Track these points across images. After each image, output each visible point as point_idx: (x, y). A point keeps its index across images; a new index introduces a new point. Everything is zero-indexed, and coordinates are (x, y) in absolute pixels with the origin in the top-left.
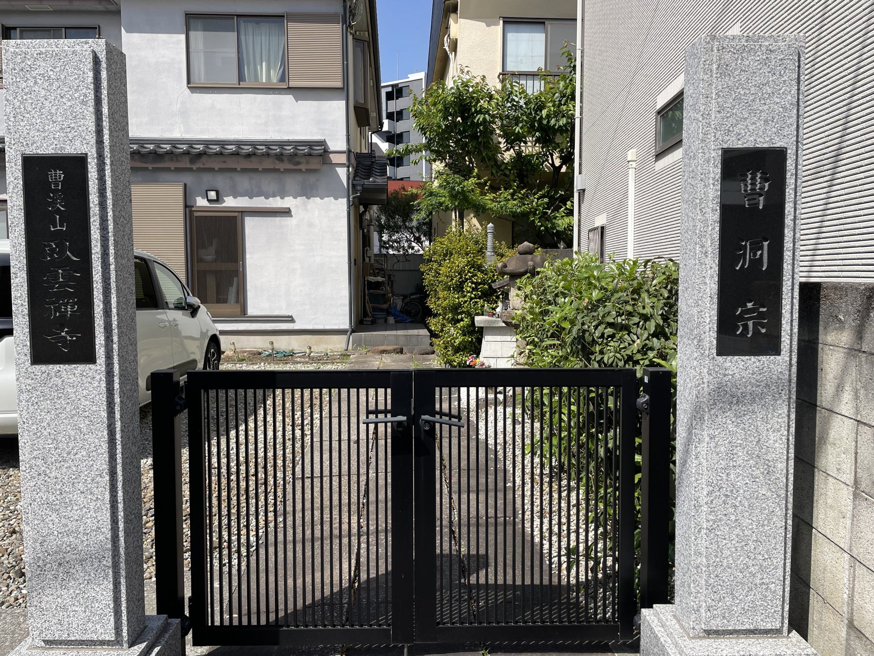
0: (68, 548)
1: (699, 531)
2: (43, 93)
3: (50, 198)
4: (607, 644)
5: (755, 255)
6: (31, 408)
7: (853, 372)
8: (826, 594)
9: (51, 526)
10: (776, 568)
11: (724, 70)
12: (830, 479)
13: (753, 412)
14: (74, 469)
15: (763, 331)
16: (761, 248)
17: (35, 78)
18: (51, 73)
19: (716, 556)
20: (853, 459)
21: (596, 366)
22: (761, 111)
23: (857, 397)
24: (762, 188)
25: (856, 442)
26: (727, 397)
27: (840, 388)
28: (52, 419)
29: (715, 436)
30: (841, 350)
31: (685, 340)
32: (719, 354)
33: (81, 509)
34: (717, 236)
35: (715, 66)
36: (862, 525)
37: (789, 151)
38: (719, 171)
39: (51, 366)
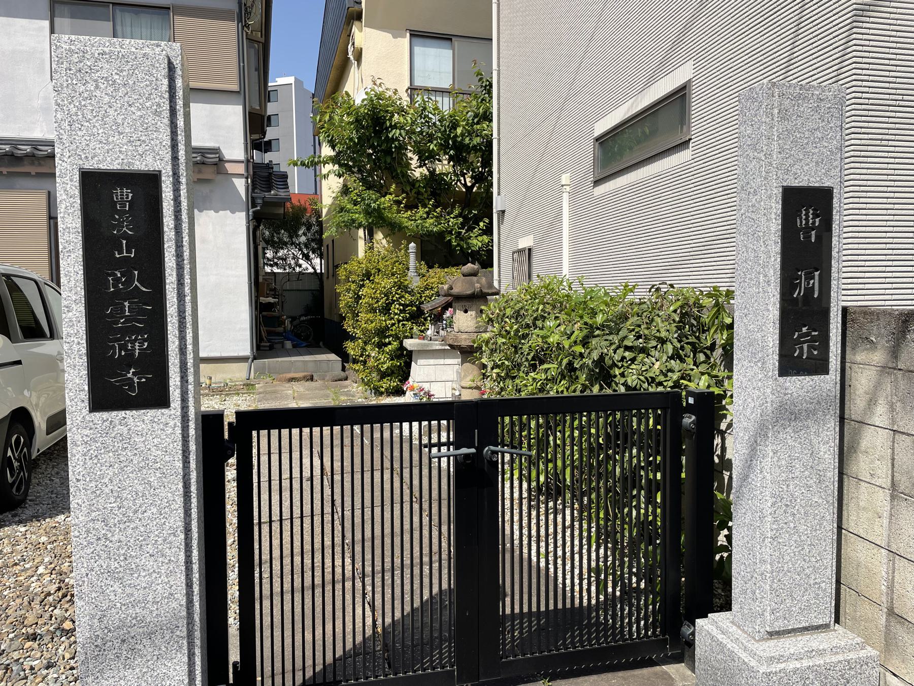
0: (134, 622)
1: (764, 540)
2: (107, 99)
3: (115, 220)
4: (650, 658)
5: (809, 284)
6: (89, 463)
7: (888, 387)
8: (861, 588)
9: (112, 597)
10: (826, 568)
11: (784, 115)
12: (863, 484)
13: (808, 427)
14: (142, 529)
15: (816, 353)
16: (813, 278)
17: (96, 81)
18: (117, 77)
19: (779, 562)
20: (890, 465)
21: (622, 390)
22: (813, 154)
23: (892, 408)
24: (814, 223)
25: (893, 449)
26: (788, 415)
27: (872, 402)
28: (115, 474)
29: (777, 451)
30: (873, 368)
31: (745, 363)
32: (781, 374)
33: (150, 575)
34: (778, 267)
35: (776, 111)
36: (902, 523)
37: (835, 191)
38: (780, 206)
39: (114, 413)
